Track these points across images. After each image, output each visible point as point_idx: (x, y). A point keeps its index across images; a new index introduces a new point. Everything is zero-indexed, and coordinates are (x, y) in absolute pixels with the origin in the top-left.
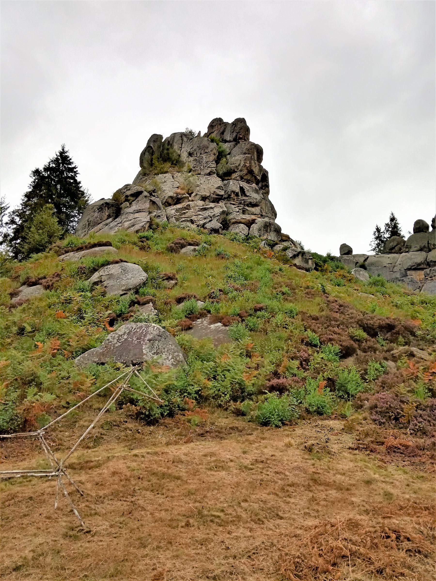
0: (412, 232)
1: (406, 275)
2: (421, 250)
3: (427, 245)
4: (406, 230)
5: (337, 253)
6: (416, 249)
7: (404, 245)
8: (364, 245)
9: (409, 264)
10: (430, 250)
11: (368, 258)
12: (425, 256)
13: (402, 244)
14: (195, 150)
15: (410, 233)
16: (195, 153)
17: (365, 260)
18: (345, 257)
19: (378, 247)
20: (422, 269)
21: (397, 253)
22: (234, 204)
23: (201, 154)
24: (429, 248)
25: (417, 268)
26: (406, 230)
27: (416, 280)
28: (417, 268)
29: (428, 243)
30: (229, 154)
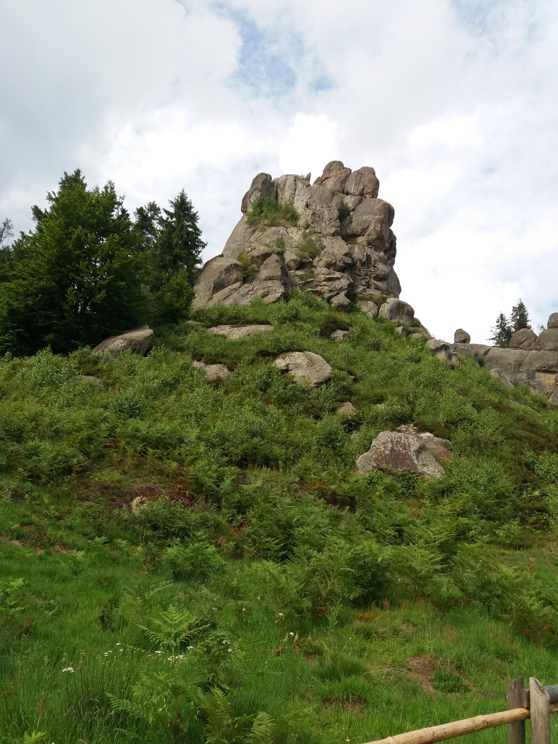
0: (546, 328)
4: (537, 323)
5: (450, 340)
7: (535, 340)
8: (483, 335)
11: (489, 350)
13: (533, 340)
14: (315, 202)
15: (542, 327)
16: (314, 205)
17: (486, 353)
18: (461, 345)
19: (499, 337)
21: (525, 349)
23: (322, 207)
26: (537, 323)
27: (545, 384)
30: (354, 210)
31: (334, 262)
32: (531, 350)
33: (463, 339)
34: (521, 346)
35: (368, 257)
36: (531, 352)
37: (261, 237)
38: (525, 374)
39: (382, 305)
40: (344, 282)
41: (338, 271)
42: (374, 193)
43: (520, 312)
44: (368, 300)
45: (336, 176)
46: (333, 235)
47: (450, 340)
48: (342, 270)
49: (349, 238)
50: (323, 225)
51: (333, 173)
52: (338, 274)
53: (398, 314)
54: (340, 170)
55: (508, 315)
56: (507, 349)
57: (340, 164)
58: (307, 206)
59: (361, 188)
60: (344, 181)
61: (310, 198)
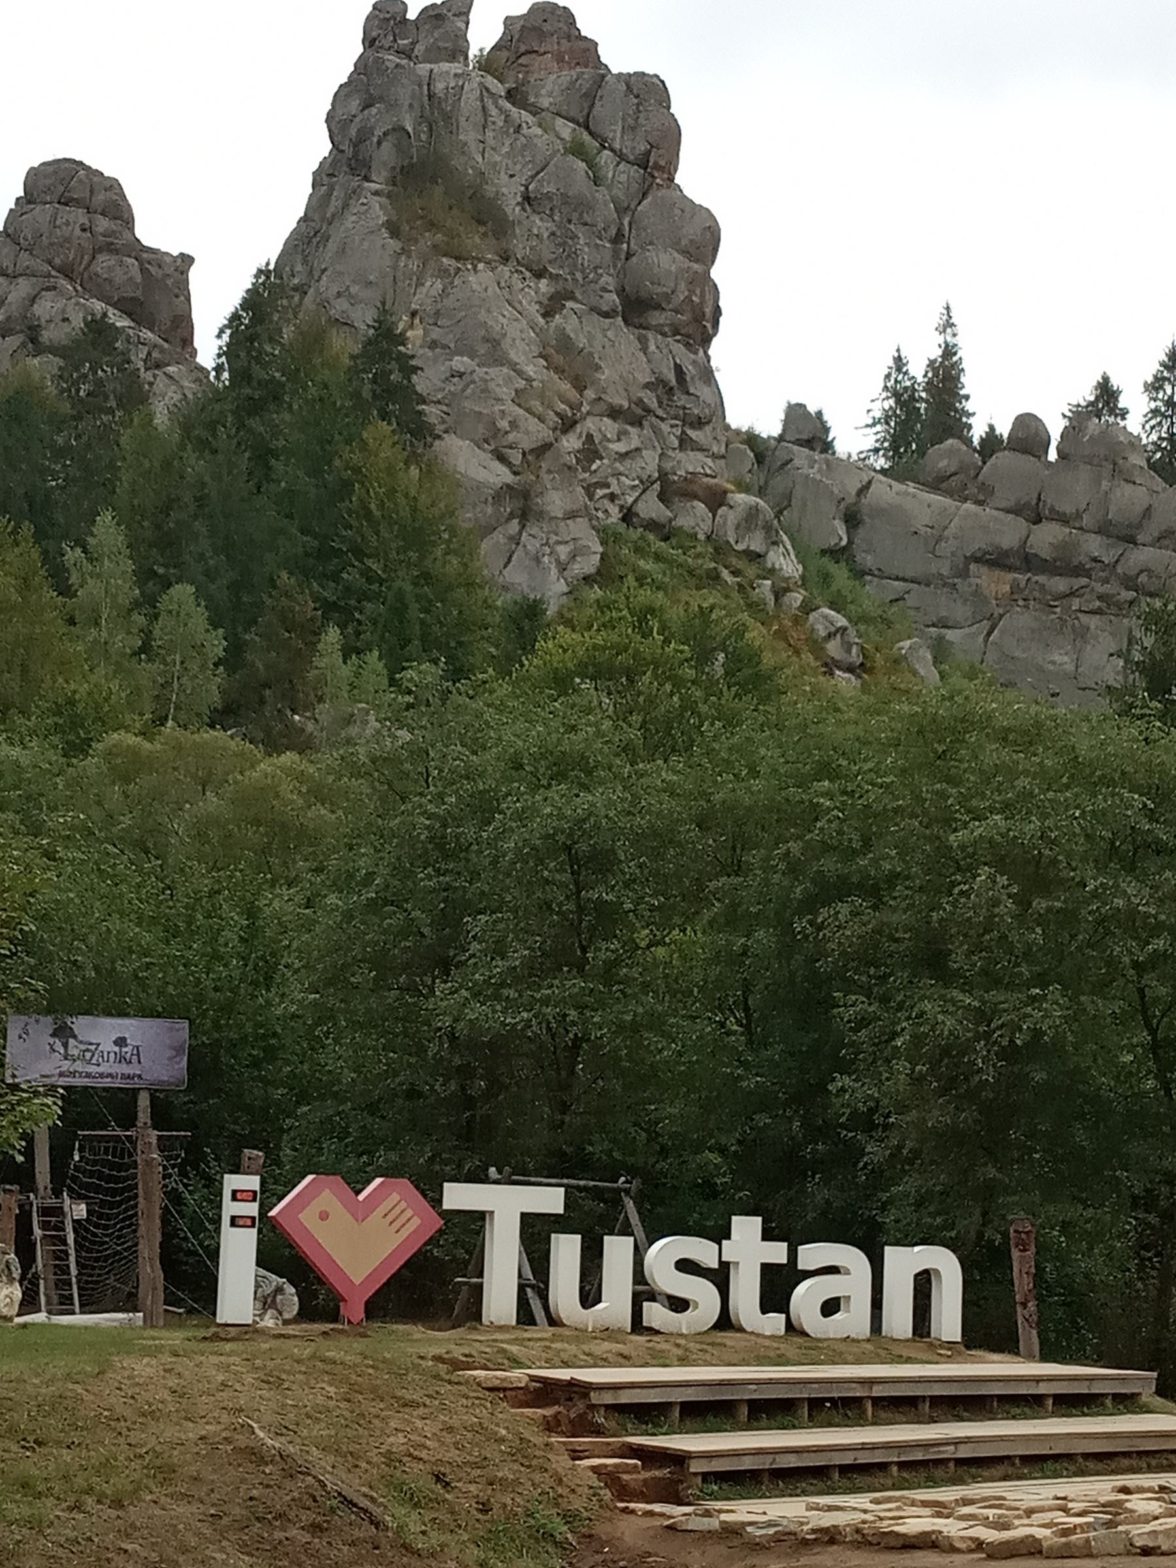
1: (964, 574)
2: (1016, 511)
3: (1034, 502)
6: (1003, 505)
9: (978, 544)
10: (1038, 520)
12: (1025, 533)
14: (548, 196)
20: (1010, 568)
22: (662, 419)
24: (1039, 515)
25: (996, 560)
28: (996, 560)
29: (1039, 499)
31: (626, 404)
32: (965, 500)
33: (806, 437)
34: (944, 485)
35: (679, 370)
36: (965, 505)
37: (449, 302)
38: (948, 563)
39: (720, 512)
40: (650, 462)
41: (632, 424)
42: (670, 167)
43: (946, 375)
44: (695, 497)
45: (560, 59)
46: (606, 315)
47: (770, 426)
48: (638, 422)
49: (636, 308)
50: (579, 276)
51: (551, 45)
52: (635, 438)
53: (749, 529)
54: (569, 38)
55: (918, 370)
56: (911, 487)
57: (567, 16)
58: (527, 198)
59: (643, 147)
60: (591, 97)
61: (533, 177)
